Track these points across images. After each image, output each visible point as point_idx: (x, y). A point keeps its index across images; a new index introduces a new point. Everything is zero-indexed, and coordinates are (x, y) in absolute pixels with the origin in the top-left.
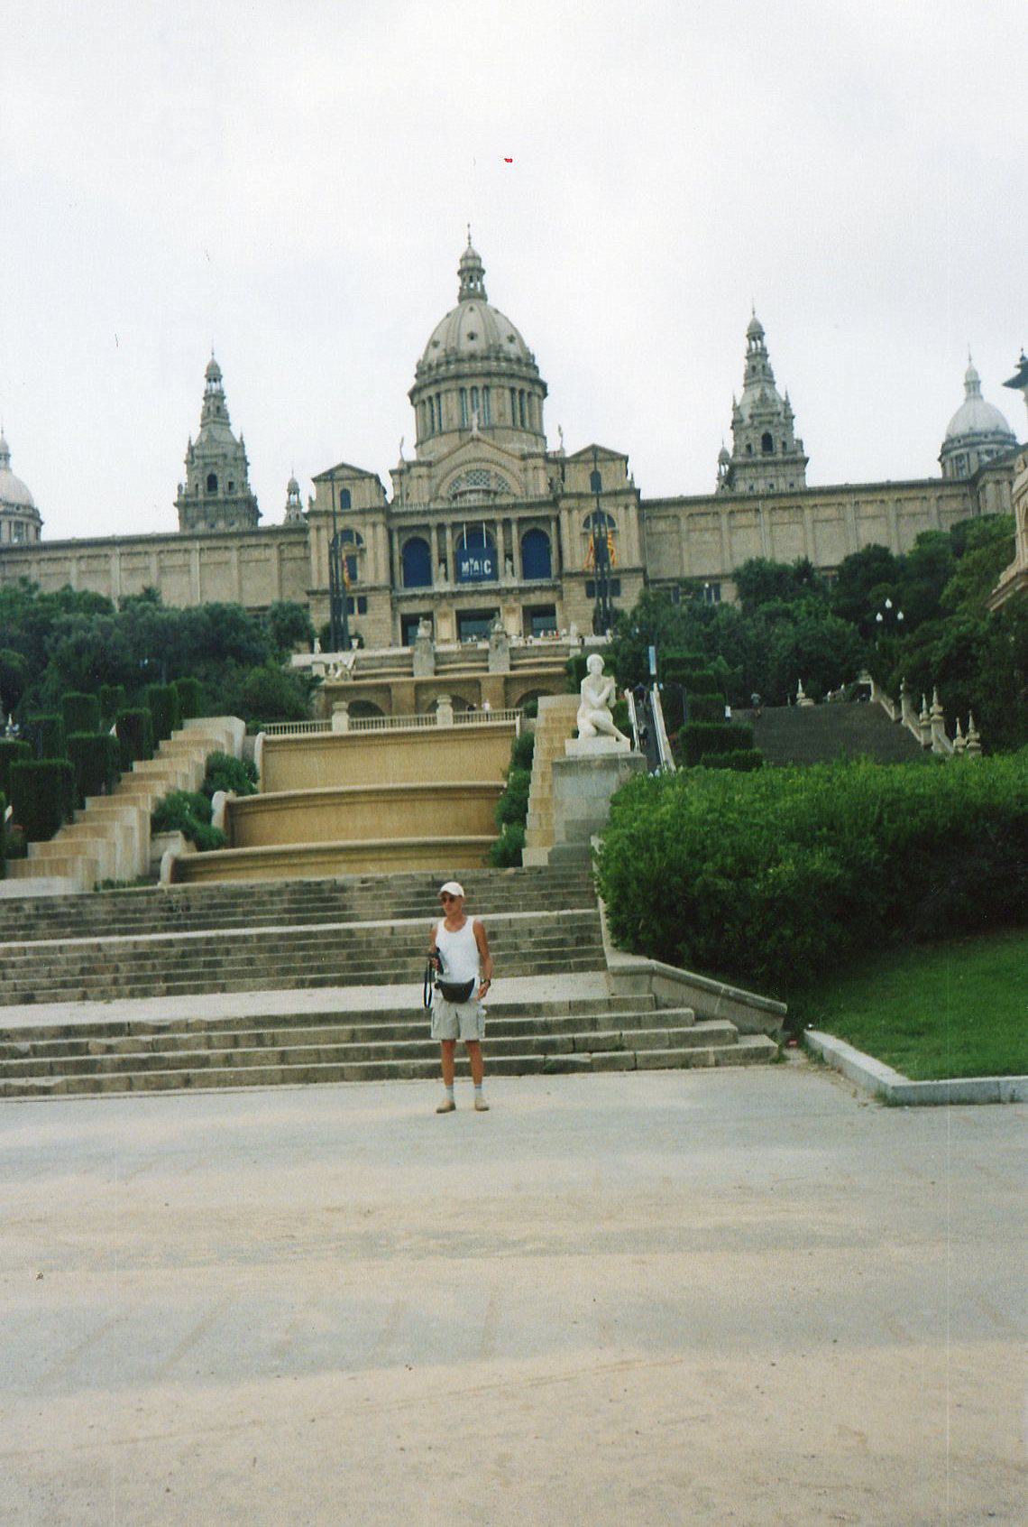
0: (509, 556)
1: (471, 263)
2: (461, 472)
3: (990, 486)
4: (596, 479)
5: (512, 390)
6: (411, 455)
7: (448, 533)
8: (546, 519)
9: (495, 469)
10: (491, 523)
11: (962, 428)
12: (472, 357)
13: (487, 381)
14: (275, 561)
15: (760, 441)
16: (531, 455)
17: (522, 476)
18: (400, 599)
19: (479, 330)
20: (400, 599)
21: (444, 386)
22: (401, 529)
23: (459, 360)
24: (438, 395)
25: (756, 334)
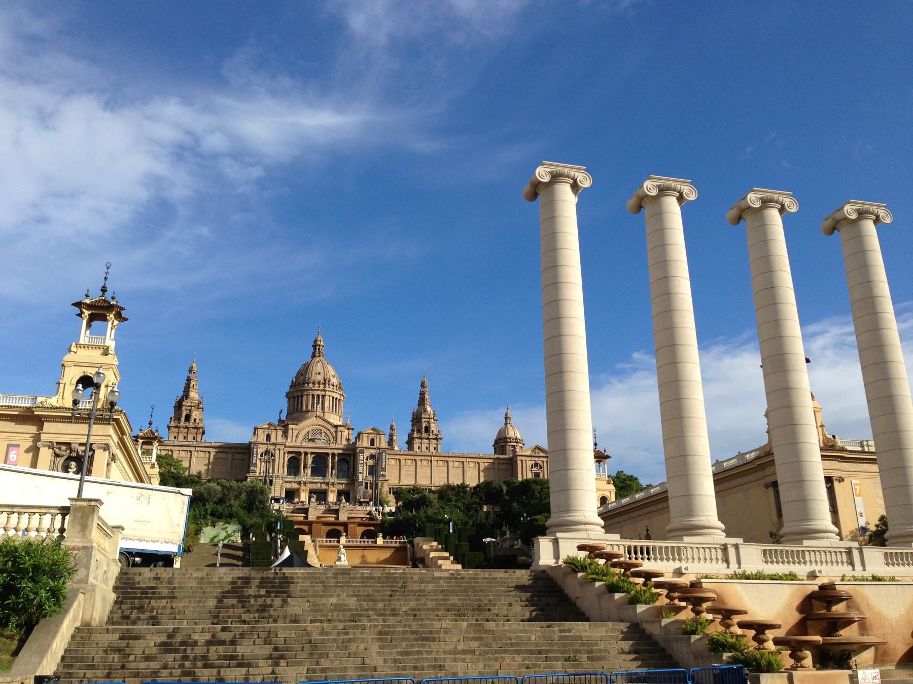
1: (318, 343)
2: (310, 429)
3: (519, 463)
6: (283, 418)
8: (349, 455)
10: (327, 454)
11: (503, 435)
13: (323, 393)
14: (230, 460)
16: (340, 426)
18: (286, 482)
20: (286, 482)
22: (289, 453)
23: (314, 383)
24: (302, 396)
25: (423, 385)
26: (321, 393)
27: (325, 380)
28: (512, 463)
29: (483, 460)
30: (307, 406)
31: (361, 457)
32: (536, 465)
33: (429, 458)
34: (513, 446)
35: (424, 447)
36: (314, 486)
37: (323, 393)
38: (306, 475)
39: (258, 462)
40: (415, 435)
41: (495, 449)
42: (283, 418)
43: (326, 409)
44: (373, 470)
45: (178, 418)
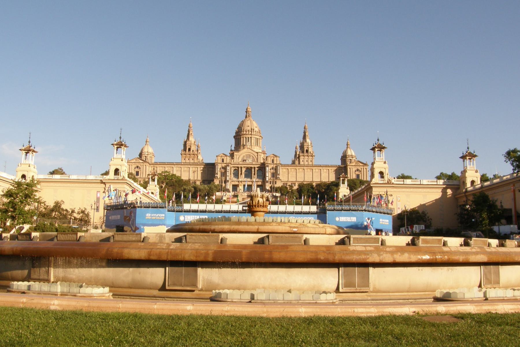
0: (254, 174)
2: (245, 154)
3: (349, 169)
4: (273, 160)
10: (251, 168)
13: (251, 136)
19: (250, 125)
26: (250, 136)
29: (331, 168)
31: (267, 169)
32: (358, 170)
34: (350, 160)
35: (305, 160)
38: (242, 178)
39: (219, 173)
42: (233, 149)
43: (252, 144)
45: (185, 150)
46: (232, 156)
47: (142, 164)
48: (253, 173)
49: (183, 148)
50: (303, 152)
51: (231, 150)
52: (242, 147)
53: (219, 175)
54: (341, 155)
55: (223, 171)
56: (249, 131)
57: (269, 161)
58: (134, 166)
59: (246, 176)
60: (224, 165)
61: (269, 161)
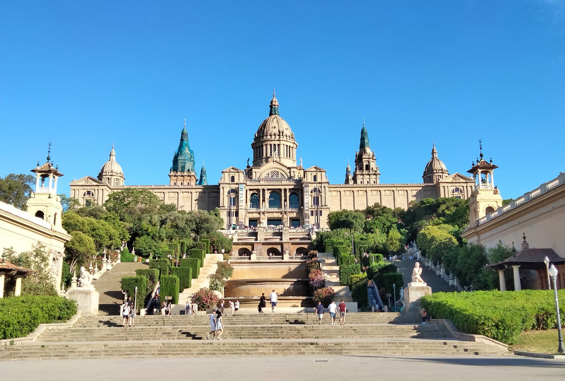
0: (285, 200)
2: (269, 171)
4: (315, 177)
5: (287, 146)
7: (266, 191)
9: (280, 171)
10: (280, 190)
12: (275, 135)
13: (278, 142)
15: (365, 167)
16: (293, 168)
17: (289, 174)
19: (276, 125)
21: (264, 144)
22: (250, 190)
23: (271, 135)
24: (262, 146)
26: (277, 143)
27: (279, 132)
28: (436, 189)
30: (266, 154)
32: (457, 190)
33: (365, 189)
36: (271, 215)
37: (278, 142)
38: (265, 206)
40: (358, 172)
41: (424, 179)
42: (251, 165)
43: (282, 155)
44: (316, 201)
46: (249, 173)
47: (96, 188)
48: (283, 198)
49: (171, 165)
50: (361, 169)
51: (248, 167)
52: (264, 162)
53: (226, 204)
54: (423, 169)
55: (233, 195)
56: (275, 135)
57: (309, 178)
58: (82, 192)
59: (271, 204)
60: (234, 187)
61: (309, 178)
